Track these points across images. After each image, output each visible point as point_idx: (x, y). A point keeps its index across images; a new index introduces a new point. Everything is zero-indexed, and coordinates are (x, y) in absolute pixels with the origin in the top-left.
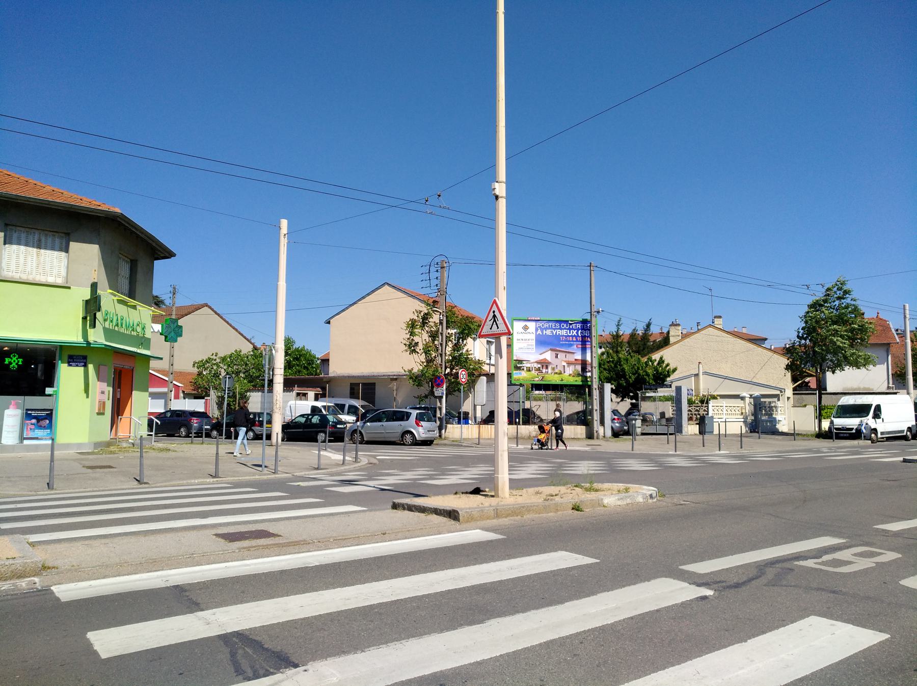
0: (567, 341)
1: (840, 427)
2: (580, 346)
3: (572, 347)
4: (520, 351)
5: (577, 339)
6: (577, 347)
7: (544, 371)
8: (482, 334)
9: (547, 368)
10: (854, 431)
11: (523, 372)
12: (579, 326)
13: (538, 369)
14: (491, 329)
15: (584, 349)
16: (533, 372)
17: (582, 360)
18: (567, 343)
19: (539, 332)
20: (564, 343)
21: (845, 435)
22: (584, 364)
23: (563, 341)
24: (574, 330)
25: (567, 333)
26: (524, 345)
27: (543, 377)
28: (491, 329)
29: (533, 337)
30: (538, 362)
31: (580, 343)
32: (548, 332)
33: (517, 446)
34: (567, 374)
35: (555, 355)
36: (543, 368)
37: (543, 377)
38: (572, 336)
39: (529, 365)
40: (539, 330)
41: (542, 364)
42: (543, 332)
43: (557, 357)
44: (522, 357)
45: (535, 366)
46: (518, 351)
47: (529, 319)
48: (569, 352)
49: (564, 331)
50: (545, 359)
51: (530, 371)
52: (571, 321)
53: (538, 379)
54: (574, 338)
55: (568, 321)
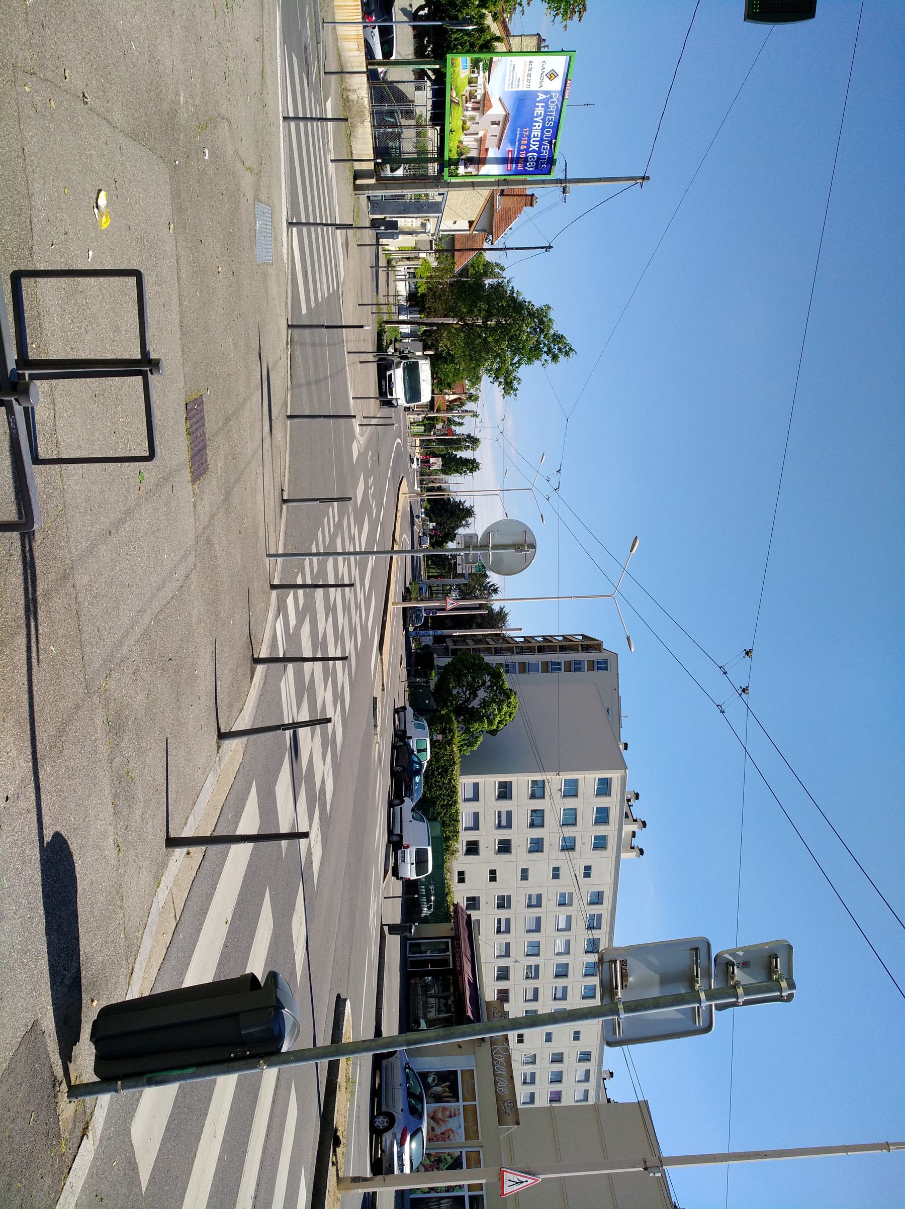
0: (522, 136)
1: (393, 380)
2: (510, 156)
3: (509, 145)
4: (508, 66)
5: (522, 151)
6: (509, 151)
7: (470, 105)
8: (505, 1173)
9: (474, 109)
10: (389, 397)
11: (468, 71)
12: (545, 154)
13: (472, 96)
14: (509, 1180)
15: (504, 161)
16: (468, 88)
17: (486, 158)
18: (518, 138)
19: (542, 97)
20: (518, 133)
21: (384, 387)
22: (479, 161)
23: (521, 131)
24: (539, 148)
25: (534, 137)
26: (520, 71)
27: (458, 103)
28: (509, 1180)
29: (534, 87)
30: (485, 96)
31: (515, 156)
32: (540, 110)
33: (332, 161)
34: (463, 138)
35: (496, 120)
36: (473, 102)
37: (458, 103)
38: (529, 143)
39: (480, 81)
40: (544, 96)
41: (482, 103)
42: (540, 102)
43: (493, 123)
44: (497, 70)
45: (479, 91)
46: (509, 62)
47: (569, 82)
48: (500, 140)
49: (540, 134)
50: (490, 106)
51: (470, 82)
52: (555, 142)
53: (454, 95)
54: (525, 147)
55: (556, 139)
